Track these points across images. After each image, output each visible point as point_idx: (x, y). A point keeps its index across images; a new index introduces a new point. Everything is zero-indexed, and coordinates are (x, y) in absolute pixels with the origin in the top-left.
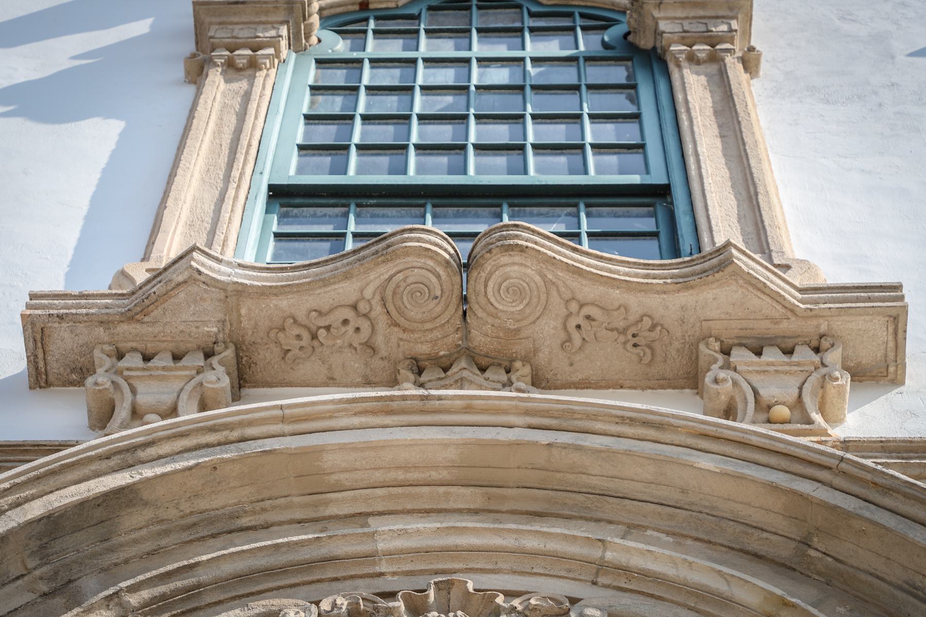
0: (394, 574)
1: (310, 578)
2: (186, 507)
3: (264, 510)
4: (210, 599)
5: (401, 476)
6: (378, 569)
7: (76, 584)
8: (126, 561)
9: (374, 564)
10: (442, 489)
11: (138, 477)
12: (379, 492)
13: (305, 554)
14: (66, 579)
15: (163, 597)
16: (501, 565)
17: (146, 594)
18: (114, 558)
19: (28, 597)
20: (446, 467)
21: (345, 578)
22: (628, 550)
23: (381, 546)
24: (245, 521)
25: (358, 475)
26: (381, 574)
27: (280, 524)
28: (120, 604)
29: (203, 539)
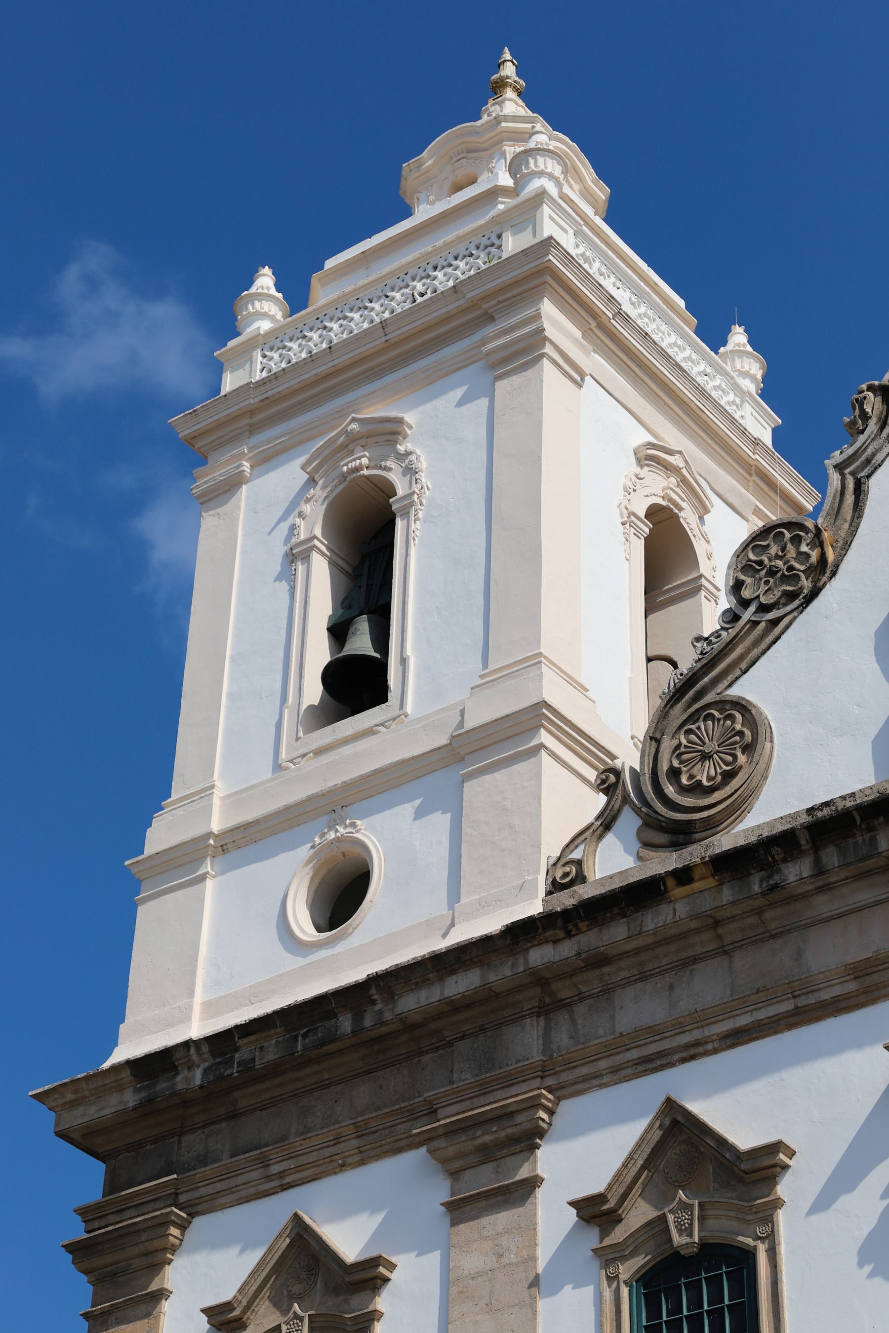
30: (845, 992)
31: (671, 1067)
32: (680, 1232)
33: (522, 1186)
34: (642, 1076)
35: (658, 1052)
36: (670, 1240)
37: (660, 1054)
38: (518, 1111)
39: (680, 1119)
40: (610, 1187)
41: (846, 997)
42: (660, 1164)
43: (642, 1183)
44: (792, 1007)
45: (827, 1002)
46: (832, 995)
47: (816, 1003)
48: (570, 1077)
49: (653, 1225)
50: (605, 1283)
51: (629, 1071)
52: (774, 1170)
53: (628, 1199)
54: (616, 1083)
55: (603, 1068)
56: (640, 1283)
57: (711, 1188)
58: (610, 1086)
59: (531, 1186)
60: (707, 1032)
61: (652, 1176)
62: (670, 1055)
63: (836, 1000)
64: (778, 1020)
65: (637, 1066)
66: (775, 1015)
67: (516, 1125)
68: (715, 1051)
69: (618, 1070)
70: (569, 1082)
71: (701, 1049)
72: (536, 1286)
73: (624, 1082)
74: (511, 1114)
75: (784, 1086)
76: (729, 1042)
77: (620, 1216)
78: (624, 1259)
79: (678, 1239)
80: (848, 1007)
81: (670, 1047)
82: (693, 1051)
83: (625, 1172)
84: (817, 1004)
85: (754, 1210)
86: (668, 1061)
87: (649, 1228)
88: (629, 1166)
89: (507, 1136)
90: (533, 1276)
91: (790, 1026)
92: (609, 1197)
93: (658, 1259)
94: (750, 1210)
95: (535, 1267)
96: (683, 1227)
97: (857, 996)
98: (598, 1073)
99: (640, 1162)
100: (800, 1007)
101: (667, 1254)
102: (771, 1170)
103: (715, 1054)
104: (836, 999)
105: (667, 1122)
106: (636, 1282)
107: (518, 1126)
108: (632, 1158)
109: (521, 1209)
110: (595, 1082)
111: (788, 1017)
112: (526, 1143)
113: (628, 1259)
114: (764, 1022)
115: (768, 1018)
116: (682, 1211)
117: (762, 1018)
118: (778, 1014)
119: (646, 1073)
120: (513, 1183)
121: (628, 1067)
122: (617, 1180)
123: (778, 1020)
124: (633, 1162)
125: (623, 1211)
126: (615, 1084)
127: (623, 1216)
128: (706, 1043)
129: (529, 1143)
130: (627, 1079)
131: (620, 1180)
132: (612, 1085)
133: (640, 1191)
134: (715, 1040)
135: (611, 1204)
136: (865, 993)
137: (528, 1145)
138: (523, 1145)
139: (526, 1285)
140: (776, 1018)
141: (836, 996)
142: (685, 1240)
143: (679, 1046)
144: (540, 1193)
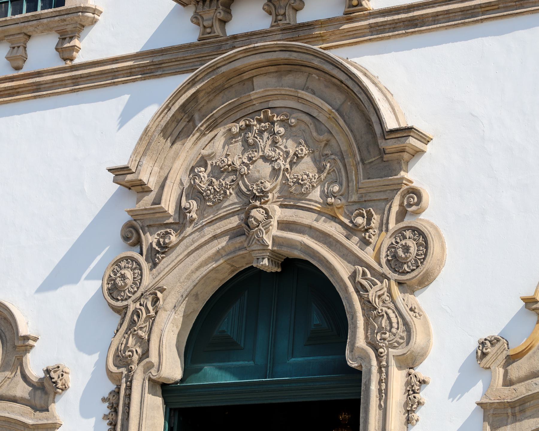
0: (257, 103)
1: (240, 109)
2: (211, 87)
3: (229, 83)
4: (219, 121)
5: (257, 65)
6: (254, 104)
7: (194, 116)
8: (203, 106)
9: (252, 102)
10: (267, 68)
11: (196, 89)
12: (253, 71)
13: (236, 104)
14: (191, 116)
15: (209, 125)
16: (279, 98)
17: (205, 126)
18: (200, 106)
19: (185, 123)
20: (266, 62)
21: (247, 107)
22: (302, 94)
23: (252, 98)
24: (226, 86)
25: (247, 67)
26: (255, 104)
27: (234, 84)
28: (200, 130)
29: (218, 94)
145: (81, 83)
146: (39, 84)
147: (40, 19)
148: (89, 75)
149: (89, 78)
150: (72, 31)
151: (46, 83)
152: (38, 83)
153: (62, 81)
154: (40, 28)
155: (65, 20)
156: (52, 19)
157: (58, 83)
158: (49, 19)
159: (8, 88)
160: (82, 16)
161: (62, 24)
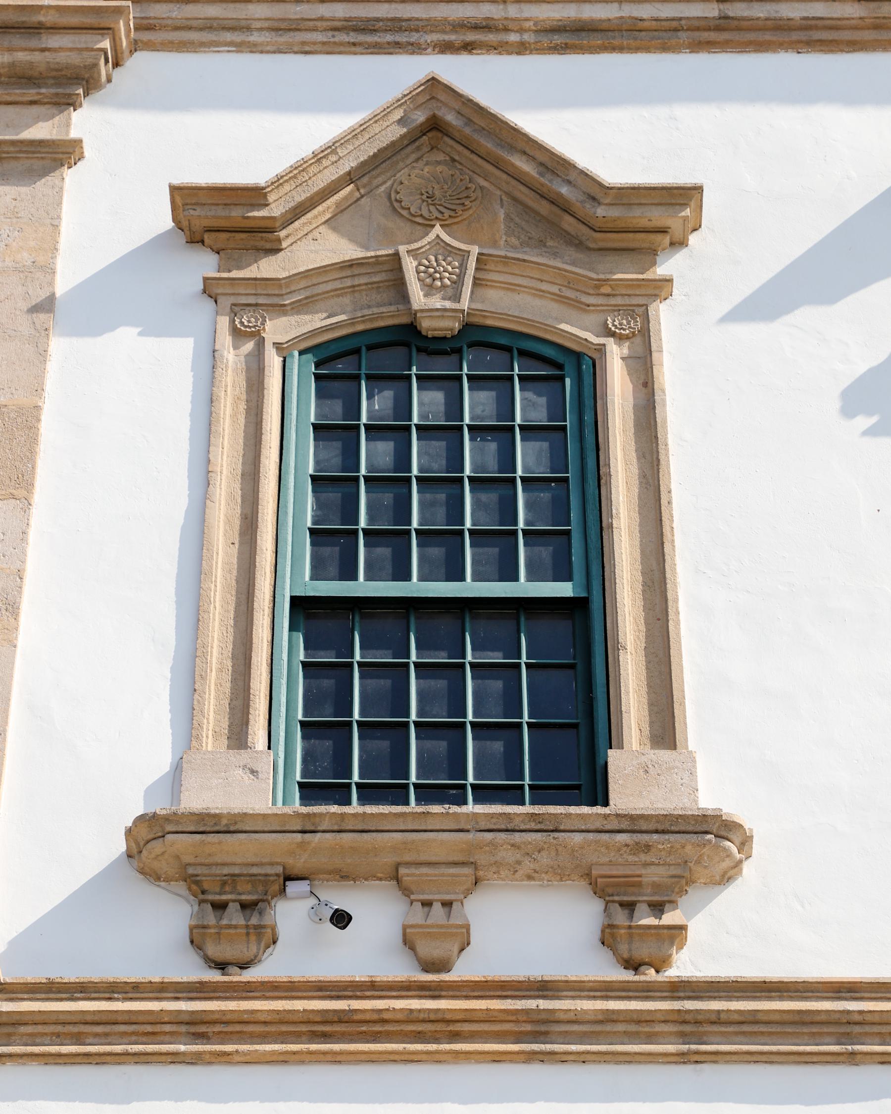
30: (835, 16)
31: (413, 53)
32: (429, 289)
33: (34, 153)
34: (340, 53)
35: (393, 20)
36: (404, 296)
37: (396, 25)
38: (55, 29)
39: (450, 118)
40: (278, 182)
41: (834, 25)
42: (377, 187)
43: (338, 204)
44: (716, 14)
45: (791, 23)
46: (806, 15)
47: (767, 19)
48: (174, 15)
49: (356, 271)
50: (225, 339)
51: (319, 37)
52: (658, 237)
53: (303, 220)
54: (280, 52)
55: (257, 16)
56: (309, 357)
57: (502, 243)
58: (262, 52)
59: (55, 160)
60: (513, 11)
61: (358, 200)
62: (417, 31)
63: (809, 25)
64: (676, 30)
65: (336, 33)
66: (673, 19)
67: (43, 50)
68: (522, 49)
69: (290, 30)
70: (169, 22)
71: (491, 37)
72: (51, 312)
73: (296, 53)
74: (37, 29)
75: (677, 129)
76: (558, 39)
77: (279, 241)
78: (281, 310)
79: (418, 297)
80: (831, 41)
81: (424, 16)
82: (471, 37)
83: (313, 169)
84: (769, 23)
85: (606, 290)
86: (412, 40)
87: (348, 272)
88: (325, 163)
89: (12, 65)
90: (43, 295)
91: (697, 46)
92: (271, 198)
93: (360, 328)
94: (597, 287)
95: (51, 283)
96: (438, 283)
97: (856, 28)
98: (243, 23)
99: (348, 165)
100: (732, 18)
101: (381, 324)
102: (652, 236)
103: (518, 53)
104: (813, 22)
105: (420, 117)
106: (301, 353)
107: (47, 53)
108: (334, 152)
109: (24, 190)
110: (229, 36)
111: (698, 29)
112: (53, 91)
113: (285, 314)
114: (646, 24)
115: (657, 20)
116: (440, 257)
117: (645, 17)
118: (680, 19)
119: (353, 49)
120: (13, 143)
121: (315, 30)
122: (295, 177)
123: (676, 30)
124: (334, 158)
125: (287, 237)
126: (274, 52)
127: (284, 245)
128: (506, 30)
129: (60, 91)
130: (307, 48)
131: (300, 179)
132: (268, 52)
133: (328, 216)
134: (526, 31)
135: (276, 209)
136: (876, 27)
137: (57, 94)
138: (43, 91)
139: (25, 306)
140: (674, 24)
141: (814, 18)
142: (437, 302)
143: (446, 19)
144: (71, 177)
145: (712, 1039)
146: (549, 1019)
147: (556, 830)
148: (752, 1019)
149: (746, 1028)
150: (657, 887)
151: (576, 1019)
152: (543, 1016)
153: (639, 1022)
154: (545, 859)
155: (648, 847)
156: (605, 837)
157: (621, 1027)
158: (591, 836)
159: (422, 1016)
160: (717, 847)
161: (631, 858)
